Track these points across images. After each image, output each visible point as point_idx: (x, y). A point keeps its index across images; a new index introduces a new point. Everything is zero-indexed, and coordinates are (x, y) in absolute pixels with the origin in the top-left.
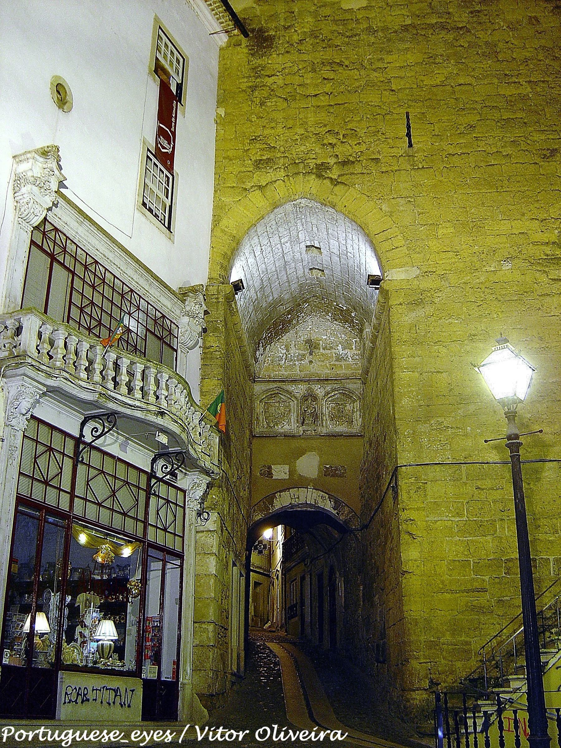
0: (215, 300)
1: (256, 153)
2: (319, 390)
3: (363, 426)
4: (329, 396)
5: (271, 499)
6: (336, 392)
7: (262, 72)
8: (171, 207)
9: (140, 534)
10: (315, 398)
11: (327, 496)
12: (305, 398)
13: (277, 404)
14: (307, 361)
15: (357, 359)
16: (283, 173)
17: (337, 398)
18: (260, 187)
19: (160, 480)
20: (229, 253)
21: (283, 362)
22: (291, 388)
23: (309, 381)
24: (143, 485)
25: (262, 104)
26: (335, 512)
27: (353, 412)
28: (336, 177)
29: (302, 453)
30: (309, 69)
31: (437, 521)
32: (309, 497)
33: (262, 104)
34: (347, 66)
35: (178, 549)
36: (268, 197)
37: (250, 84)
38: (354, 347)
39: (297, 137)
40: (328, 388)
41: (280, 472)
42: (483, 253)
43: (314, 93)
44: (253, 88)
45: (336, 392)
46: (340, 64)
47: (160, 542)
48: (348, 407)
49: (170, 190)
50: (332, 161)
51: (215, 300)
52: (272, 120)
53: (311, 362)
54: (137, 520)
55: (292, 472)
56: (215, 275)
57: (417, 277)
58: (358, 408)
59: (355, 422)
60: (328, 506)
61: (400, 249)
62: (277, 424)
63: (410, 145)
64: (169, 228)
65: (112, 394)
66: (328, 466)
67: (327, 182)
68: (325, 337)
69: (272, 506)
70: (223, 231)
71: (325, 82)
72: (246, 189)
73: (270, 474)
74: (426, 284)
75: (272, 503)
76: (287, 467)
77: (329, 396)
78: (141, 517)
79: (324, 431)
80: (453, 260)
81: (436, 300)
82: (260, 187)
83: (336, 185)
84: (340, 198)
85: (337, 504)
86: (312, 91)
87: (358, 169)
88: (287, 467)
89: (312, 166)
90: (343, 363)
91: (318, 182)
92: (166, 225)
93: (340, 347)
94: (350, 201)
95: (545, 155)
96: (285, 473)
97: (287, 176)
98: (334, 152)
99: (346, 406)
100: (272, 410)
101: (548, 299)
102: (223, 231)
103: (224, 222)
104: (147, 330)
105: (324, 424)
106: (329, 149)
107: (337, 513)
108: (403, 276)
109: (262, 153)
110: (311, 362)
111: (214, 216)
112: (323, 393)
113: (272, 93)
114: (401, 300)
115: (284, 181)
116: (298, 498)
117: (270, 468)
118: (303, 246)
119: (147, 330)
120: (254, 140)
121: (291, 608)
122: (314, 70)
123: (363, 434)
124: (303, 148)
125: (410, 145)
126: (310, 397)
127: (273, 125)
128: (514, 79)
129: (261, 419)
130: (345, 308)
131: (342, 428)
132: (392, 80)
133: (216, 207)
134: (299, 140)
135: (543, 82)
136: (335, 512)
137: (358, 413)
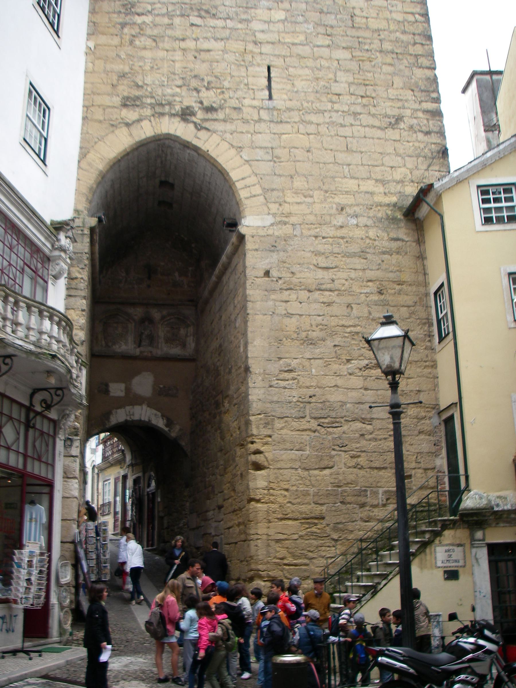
0: (80, 232)
1: (124, 90)
2: (156, 314)
3: (197, 350)
5: (107, 415)
7: (133, 10)
8: (46, 140)
9: (20, 466)
11: (159, 414)
16: (148, 112)
18: (128, 125)
19: (37, 413)
20: (95, 186)
22: (131, 310)
24: (23, 419)
25: (131, 42)
26: (166, 429)
27: (187, 336)
28: (198, 121)
29: (137, 373)
30: (178, 13)
31: (283, 455)
32: (142, 413)
33: (131, 42)
34: (214, 15)
35: (50, 477)
36: (134, 135)
37: (121, 20)
38: (190, 275)
39: (163, 79)
40: (165, 312)
41: (117, 390)
42: (332, 208)
43: (181, 37)
44: (123, 25)
46: (207, 12)
47: (36, 472)
48: (182, 332)
49: (46, 121)
50: (196, 107)
51: (80, 232)
52: (142, 58)
53: (149, 286)
54: (18, 452)
55: (128, 390)
56: (80, 207)
57: (272, 225)
60: (160, 423)
61: (258, 197)
63: (270, 97)
64: (44, 161)
65: (10, 338)
66: (161, 386)
67: (191, 126)
68: (162, 264)
69: (109, 421)
70: (89, 164)
71: (194, 28)
72: (113, 125)
73: (107, 391)
74: (278, 231)
75: (108, 419)
76: (123, 386)
78: (21, 450)
80: (305, 212)
81: (290, 249)
82: (128, 125)
83: (199, 130)
84: (202, 142)
85: (169, 423)
86: (178, 33)
87: (220, 115)
88: (123, 386)
89: (178, 108)
91: (183, 125)
92: (42, 157)
93: (177, 274)
94: (213, 147)
95: (390, 123)
96: (122, 391)
97: (153, 116)
98: (199, 97)
101: (386, 256)
102: (89, 164)
103: (91, 156)
104: (25, 264)
106: (195, 94)
107: (169, 430)
108: (259, 223)
109: (129, 90)
110: (149, 286)
111: (81, 148)
113: (141, 32)
114: (257, 247)
115: (150, 121)
116: (133, 415)
117: (107, 385)
118: (157, 181)
119: (25, 264)
120: (123, 76)
121: (103, 505)
122: (182, 15)
124: (169, 91)
125: (270, 97)
127: (141, 64)
128: (366, 47)
130: (186, 239)
131: (175, 351)
132: (257, 34)
133: (83, 140)
134: (166, 83)
135: (393, 53)
136: (166, 429)
137: (192, 338)
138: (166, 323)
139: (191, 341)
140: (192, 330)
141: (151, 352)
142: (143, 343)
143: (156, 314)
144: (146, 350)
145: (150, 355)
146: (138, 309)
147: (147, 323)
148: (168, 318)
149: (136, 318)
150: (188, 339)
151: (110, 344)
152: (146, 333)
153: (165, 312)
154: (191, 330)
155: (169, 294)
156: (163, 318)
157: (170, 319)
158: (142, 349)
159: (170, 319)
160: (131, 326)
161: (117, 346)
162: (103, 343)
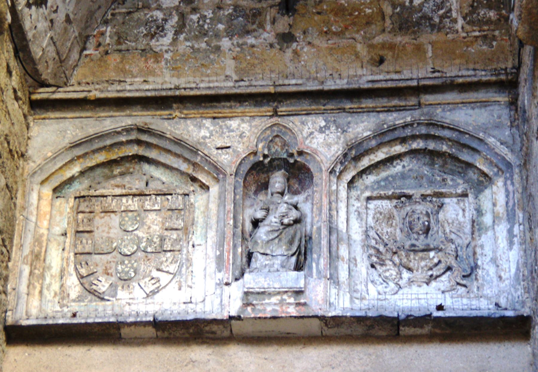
4: (365, 162)
6: (398, 149)
10: (298, 172)
12: (257, 173)
13: (133, 204)
14: (268, 35)
15: (489, 22)
17: (403, 176)
21: (167, 40)
22: (198, 130)
23: (271, 99)
27: (476, 226)
45: (398, 149)
58: (501, 209)
59: (486, 270)
62: (126, 280)
77: (365, 162)
79: (342, 305)
90: (427, 38)
99: (441, 206)
100: (107, 228)
105: (343, 275)
110: (286, 38)
112: (337, 150)
123: (526, 311)
126: (278, 169)
129: (55, 258)
137: (502, 229)
138: (370, 179)
139: (503, 243)
140: (501, 198)
141: (299, 293)
142: (259, 261)
143: (320, 138)
144: (273, 279)
145: (292, 311)
146: (234, 123)
147: (278, 180)
148: (381, 155)
149: (225, 159)
150: (485, 239)
151: (103, 286)
152: (273, 219)
153: (362, 127)
154: (497, 195)
155: (381, 61)
156: (354, 152)
157: (390, 160)
158: (252, 281)
159: (390, 160)
160: (208, 206)
161: (138, 293)
162: (72, 281)
